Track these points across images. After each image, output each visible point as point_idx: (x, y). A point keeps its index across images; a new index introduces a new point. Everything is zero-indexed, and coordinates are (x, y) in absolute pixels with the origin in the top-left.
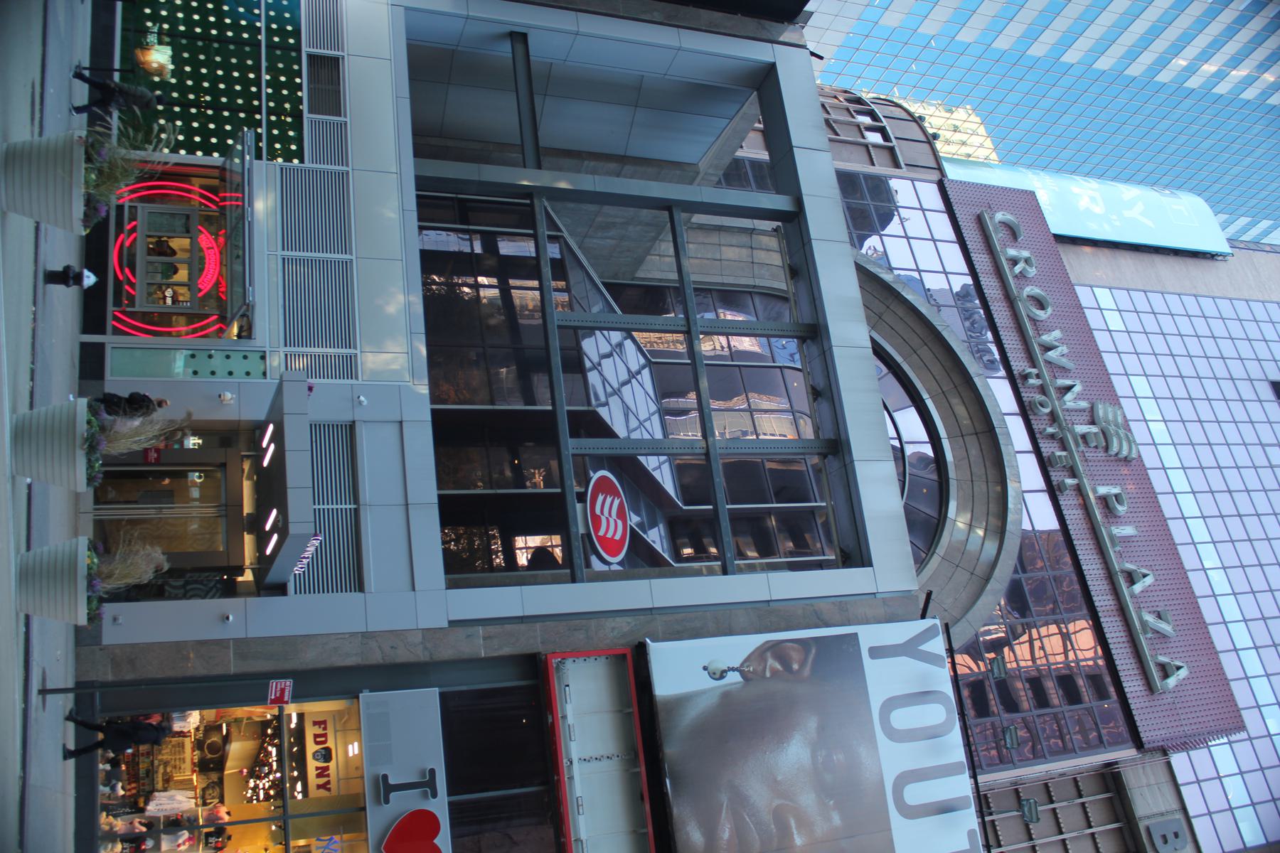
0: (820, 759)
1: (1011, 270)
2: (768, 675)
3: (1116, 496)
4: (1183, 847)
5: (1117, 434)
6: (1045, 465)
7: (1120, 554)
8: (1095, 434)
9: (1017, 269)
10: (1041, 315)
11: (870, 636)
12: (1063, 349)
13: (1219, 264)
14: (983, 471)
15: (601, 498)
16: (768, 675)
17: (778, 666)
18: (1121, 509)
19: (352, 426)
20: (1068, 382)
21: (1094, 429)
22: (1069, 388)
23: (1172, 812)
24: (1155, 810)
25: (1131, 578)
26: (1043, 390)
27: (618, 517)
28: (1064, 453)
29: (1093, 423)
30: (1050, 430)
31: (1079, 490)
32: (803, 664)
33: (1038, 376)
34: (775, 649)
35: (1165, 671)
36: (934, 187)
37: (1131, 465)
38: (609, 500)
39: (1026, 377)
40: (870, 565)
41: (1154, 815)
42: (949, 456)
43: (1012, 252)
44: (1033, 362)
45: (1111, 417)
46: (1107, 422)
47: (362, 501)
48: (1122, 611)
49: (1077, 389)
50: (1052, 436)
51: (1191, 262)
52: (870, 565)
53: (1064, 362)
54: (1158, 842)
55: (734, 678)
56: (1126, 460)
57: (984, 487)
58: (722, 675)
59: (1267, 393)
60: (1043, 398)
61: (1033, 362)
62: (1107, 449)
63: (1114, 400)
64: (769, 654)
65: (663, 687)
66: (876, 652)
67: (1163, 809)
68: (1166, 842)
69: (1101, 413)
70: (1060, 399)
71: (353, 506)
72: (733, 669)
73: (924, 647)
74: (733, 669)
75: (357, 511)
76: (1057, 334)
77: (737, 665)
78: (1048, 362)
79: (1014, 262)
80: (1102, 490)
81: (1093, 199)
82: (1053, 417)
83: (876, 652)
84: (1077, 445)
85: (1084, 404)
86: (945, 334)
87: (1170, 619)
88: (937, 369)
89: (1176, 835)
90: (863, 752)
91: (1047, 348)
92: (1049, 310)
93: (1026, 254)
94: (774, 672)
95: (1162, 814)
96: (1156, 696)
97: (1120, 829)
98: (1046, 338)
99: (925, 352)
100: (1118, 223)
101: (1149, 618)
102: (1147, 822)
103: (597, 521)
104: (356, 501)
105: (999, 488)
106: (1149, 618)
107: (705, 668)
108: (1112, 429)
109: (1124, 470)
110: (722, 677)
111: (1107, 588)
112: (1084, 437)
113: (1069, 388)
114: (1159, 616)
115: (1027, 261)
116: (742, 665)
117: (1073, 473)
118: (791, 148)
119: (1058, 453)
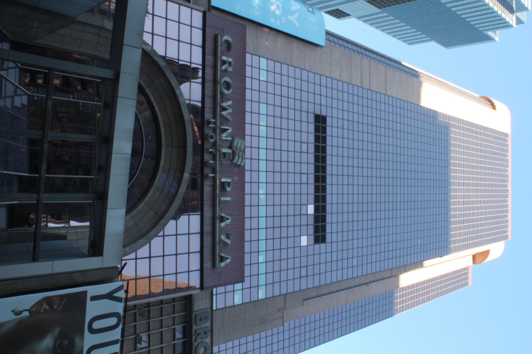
0: (57, 344)
1: (221, 66)
2: (42, 311)
3: (228, 183)
4: (207, 322)
5: (239, 153)
7: (221, 209)
8: (229, 153)
9: (224, 67)
10: (226, 92)
11: (92, 290)
12: (230, 111)
13: (319, 49)
16: (42, 311)
17: (48, 307)
18: (228, 189)
20: (226, 128)
21: (230, 151)
22: (226, 130)
24: (201, 308)
25: (222, 219)
26: (214, 130)
28: (213, 162)
29: (230, 147)
30: (211, 150)
31: (214, 179)
33: (215, 123)
34: (47, 300)
35: (222, 259)
36: (200, 15)
37: (241, 169)
39: (209, 122)
41: (200, 310)
43: (224, 58)
44: (215, 117)
45: (239, 146)
46: (236, 148)
49: (229, 131)
50: (211, 152)
51: (307, 45)
53: (228, 117)
54: (198, 320)
55: (26, 314)
56: (239, 166)
58: (21, 313)
59: (312, 119)
60: (213, 134)
61: (215, 117)
62: (232, 160)
63: (243, 136)
64: (44, 303)
66: (93, 298)
68: (201, 319)
69: (235, 144)
72: (26, 310)
73: (116, 295)
74: (26, 310)
76: (230, 103)
77: (28, 308)
78: (221, 116)
79: (224, 62)
80: (223, 180)
81: (278, 7)
82: (214, 144)
83: (93, 298)
84: (220, 158)
85: (230, 139)
87: (231, 238)
89: (206, 318)
90: (77, 340)
91: (224, 109)
92: (231, 91)
93: (230, 60)
94: (45, 310)
95: (203, 310)
97: (186, 314)
98: (224, 104)
100: (284, 22)
101: (223, 237)
105: (179, 175)
106: (223, 237)
107: (13, 311)
108: (237, 152)
109: (236, 170)
111: (211, 223)
112: (224, 154)
113: (226, 130)
114: (228, 237)
115: (230, 63)
116: (31, 308)
117: (214, 171)
119: (211, 162)
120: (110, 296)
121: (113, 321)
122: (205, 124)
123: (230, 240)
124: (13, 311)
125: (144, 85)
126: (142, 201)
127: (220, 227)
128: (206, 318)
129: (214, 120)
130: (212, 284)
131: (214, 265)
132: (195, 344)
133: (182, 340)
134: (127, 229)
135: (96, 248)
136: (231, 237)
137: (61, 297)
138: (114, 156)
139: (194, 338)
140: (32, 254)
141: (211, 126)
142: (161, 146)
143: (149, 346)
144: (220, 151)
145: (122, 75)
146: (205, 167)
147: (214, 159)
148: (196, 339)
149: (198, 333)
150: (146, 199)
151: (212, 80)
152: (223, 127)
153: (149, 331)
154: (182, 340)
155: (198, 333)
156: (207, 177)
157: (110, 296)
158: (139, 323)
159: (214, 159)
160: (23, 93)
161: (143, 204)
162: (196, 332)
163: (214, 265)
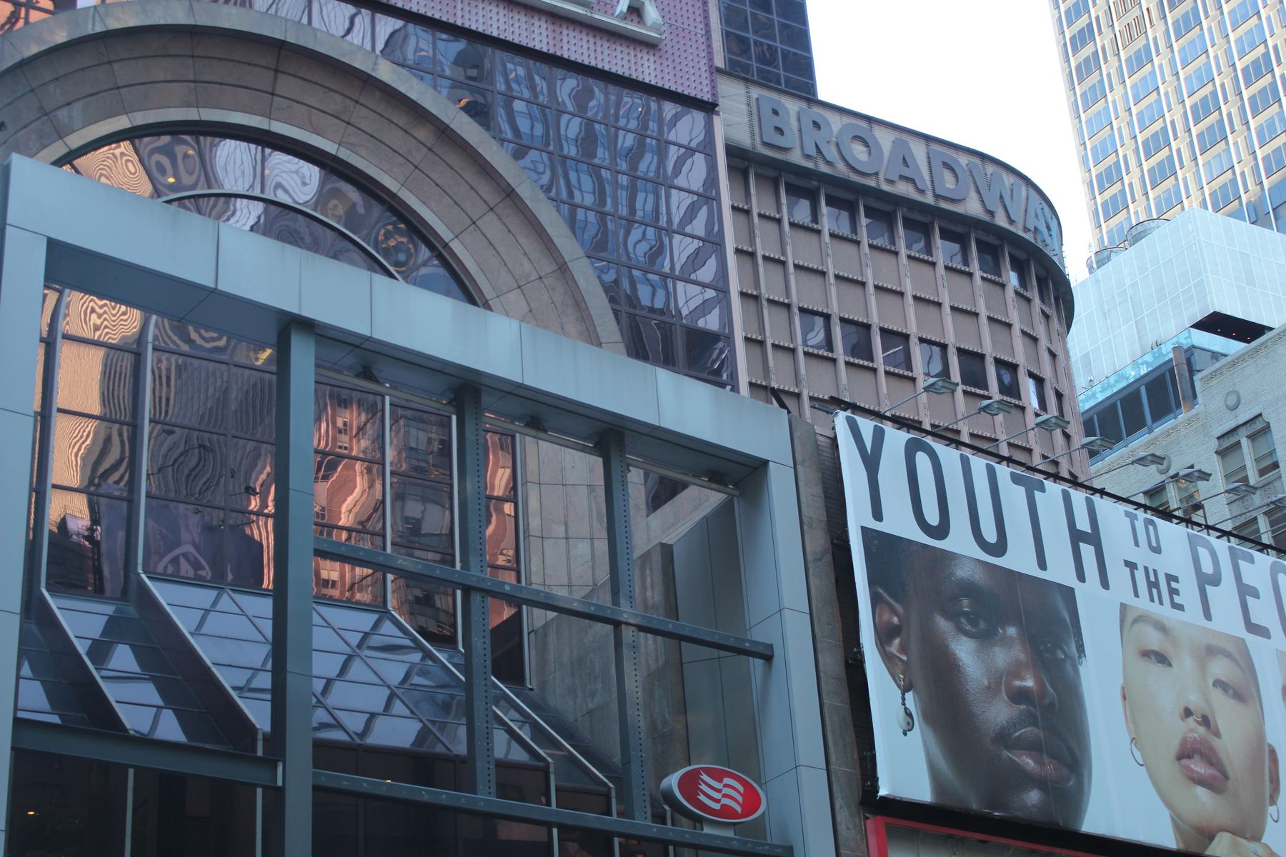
0: (969, 628)
2: (905, 658)
14: (339, 98)
15: (702, 798)
16: (905, 658)
17: (897, 641)
24: (747, 120)
32: (895, 613)
34: (884, 636)
38: (703, 787)
42: (329, 147)
52: (765, 463)
54: (780, 141)
57: (364, 112)
65: (921, 791)
67: (745, 107)
68: (779, 130)
72: (904, 699)
74: (904, 699)
77: (899, 692)
86: (114, 24)
88: (160, 70)
94: (903, 649)
95: (750, 114)
97: (756, 175)
99: (124, 73)
103: (726, 811)
107: (905, 734)
110: (909, 714)
116: (899, 686)
118: (214, 292)
120: (871, 462)
121: (922, 459)
124: (905, 734)
125: (58, 149)
126: (446, 245)
128: (775, 112)
130: (704, 68)
131: (650, 45)
132: (841, 170)
133: (864, 221)
134: (532, 316)
135: (739, 475)
137: (876, 600)
138: (530, 381)
139: (824, 168)
140: (723, 653)
142: (268, 133)
143: (827, 317)
145: (307, 313)
148: (829, 163)
149: (813, 152)
153: (788, 306)
154: (864, 221)
155: (813, 152)
157: (871, 462)
158: (768, 333)
160: (408, 642)
161: (456, 246)
162: (808, 157)
163: (650, 45)
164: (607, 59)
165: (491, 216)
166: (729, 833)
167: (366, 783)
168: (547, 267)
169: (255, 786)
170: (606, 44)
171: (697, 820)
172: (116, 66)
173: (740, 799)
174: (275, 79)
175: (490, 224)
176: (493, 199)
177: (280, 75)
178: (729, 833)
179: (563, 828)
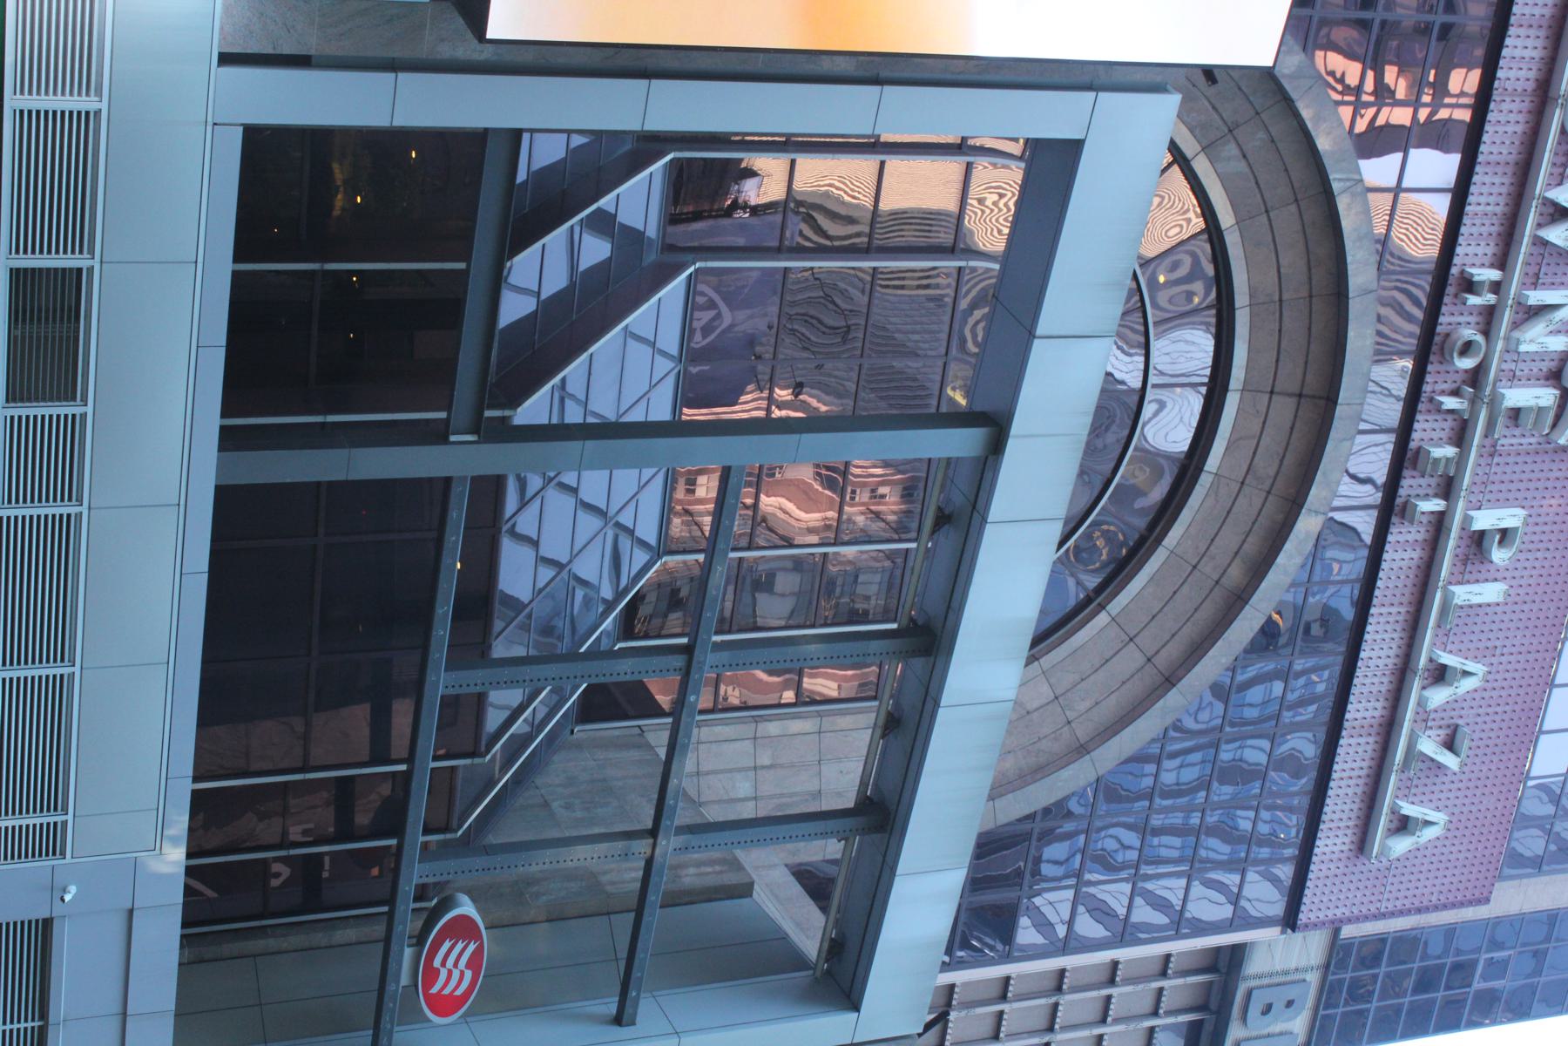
4: (1290, 1019)
6: (1404, 457)
8: (1541, 410)
14: (1272, 472)
15: (447, 945)
18: (1499, 555)
19: (47, 923)
23: (1305, 970)
24: (1278, 968)
27: (468, 966)
31: (1440, 523)
38: (460, 946)
39: (1469, 286)
40: (856, 1008)
42: (1213, 462)
44: (1502, 261)
47: (52, 1019)
48: (1389, 728)
52: (856, 1008)
57: (1257, 502)
60: (1479, 338)
61: (1502, 261)
67: (1293, 966)
68: (1267, 1009)
70: (1516, 325)
71: (36, 1024)
75: (42, 1032)
82: (1476, 377)
86: (1342, 203)
87: (1464, 751)
88: (1292, 260)
95: (1286, 973)
96: (1363, 859)
99: (1286, 218)
101: (1429, 746)
102: (1253, 983)
103: (431, 975)
104: (44, 1015)
106: (1429, 746)
112: (1516, 414)
114: (1450, 745)
117: (1447, 488)
118: (1031, 335)
122: (1450, 290)
123: (1457, 754)
125: (1189, 146)
126: (1102, 607)
127: (1421, 703)
128: (1290, 1004)
129: (1495, 275)
130: (1338, 912)
131: (1362, 843)
134: (1022, 715)
136: (1464, 745)
141: (1473, 300)
142: (1225, 389)
144: (1495, 400)
145: (1014, 448)
146: (1406, 473)
147: (1460, 437)
150: (1117, 605)
151: (1530, 86)
152: (1535, 297)
153: (1051, 1029)
156: (1406, 512)
158: (1016, 1005)
159: (1460, 437)
160: (624, 582)
161: (1102, 619)
163: (1362, 843)
164: (1340, 792)
165: (1141, 660)
166: (405, 980)
167: (455, 539)
168: (1083, 732)
169: (449, 408)
170: (1359, 790)
171: (420, 940)
172: (1293, 208)
173: (446, 992)
174: (1290, 395)
175: (1131, 659)
176: (1161, 661)
177: (1295, 400)
178: (405, 980)
179: (407, 776)
